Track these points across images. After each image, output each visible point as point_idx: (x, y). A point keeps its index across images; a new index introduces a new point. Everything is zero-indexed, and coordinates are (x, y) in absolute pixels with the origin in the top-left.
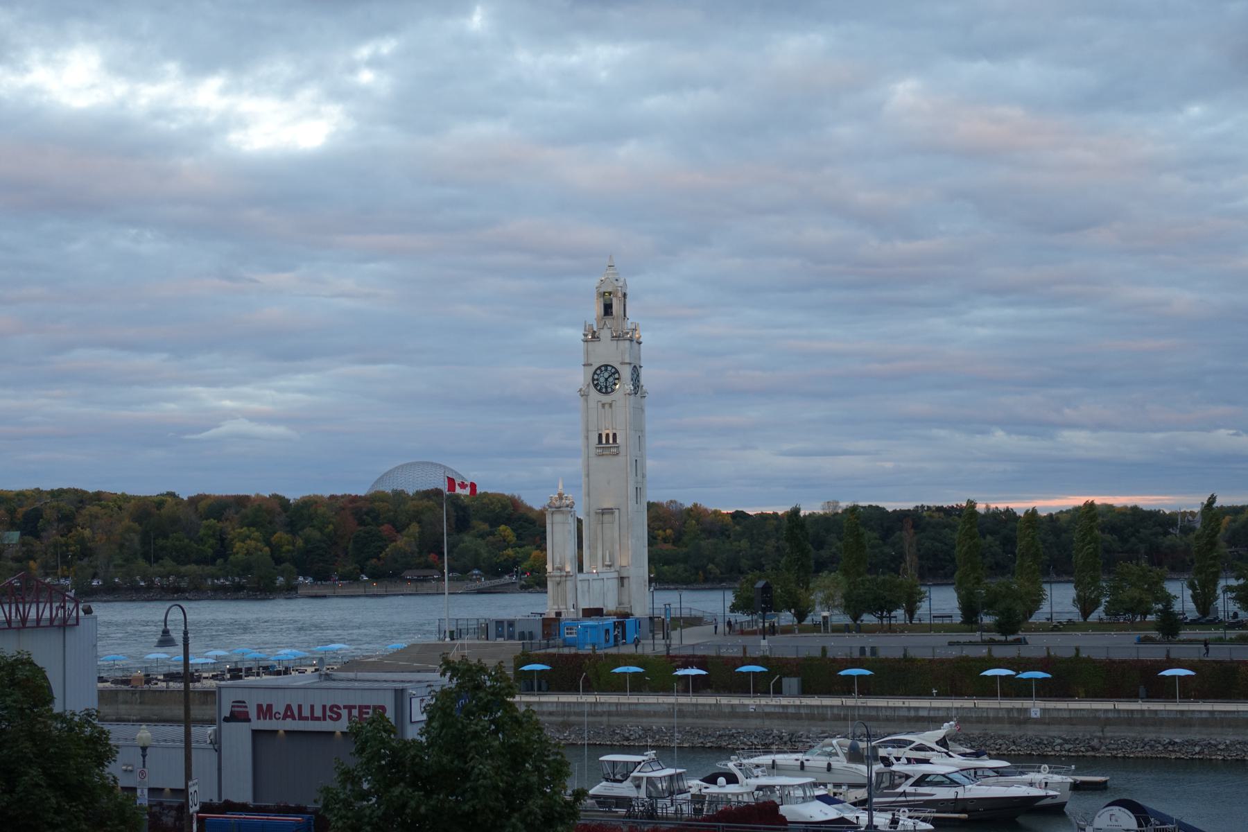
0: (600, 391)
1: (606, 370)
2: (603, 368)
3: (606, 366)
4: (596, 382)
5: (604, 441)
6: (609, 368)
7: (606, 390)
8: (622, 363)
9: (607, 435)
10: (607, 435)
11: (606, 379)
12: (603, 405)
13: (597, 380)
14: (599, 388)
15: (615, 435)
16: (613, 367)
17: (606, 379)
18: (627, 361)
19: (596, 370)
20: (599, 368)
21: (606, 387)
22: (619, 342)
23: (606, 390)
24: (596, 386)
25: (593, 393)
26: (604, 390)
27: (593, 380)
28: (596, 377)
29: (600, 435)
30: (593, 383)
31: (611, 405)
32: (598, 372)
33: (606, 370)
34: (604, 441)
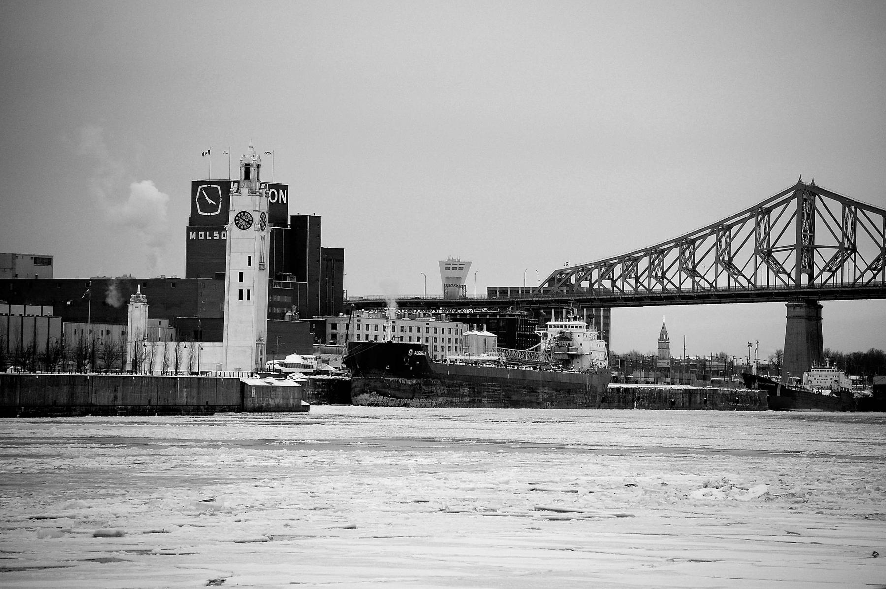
0: (239, 228)
1: (244, 215)
2: (242, 213)
3: (244, 212)
4: (237, 222)
6: (246, 214)
7: (243, 227)
8: (254, 211)
11: (244, 220)
14: (239, 226)
16: (248, 213)
18: (258, 209)
20: (240, 213)
21: (244, 226)
23: (243, 227)
24: (237, 224)
26: (242, 228)
27: (235, 220)
30: (235, 222)
33: (244, 215)
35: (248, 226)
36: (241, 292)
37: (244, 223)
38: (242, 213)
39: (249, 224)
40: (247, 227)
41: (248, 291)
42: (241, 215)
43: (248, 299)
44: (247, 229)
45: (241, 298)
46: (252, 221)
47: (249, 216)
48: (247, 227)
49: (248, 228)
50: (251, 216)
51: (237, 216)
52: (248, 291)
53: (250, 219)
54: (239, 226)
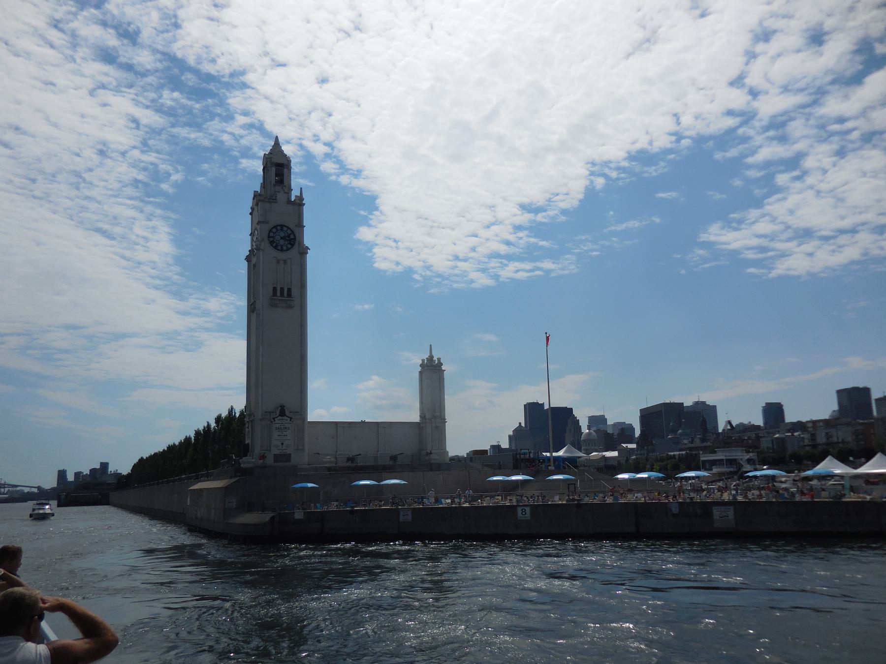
0: (275, 248)
1: (282, 230)
3: (282, 226)
4: (271, 239)
5: (278, 294)
6: (285, 229)
7: (282, 248)
9: (282, 289)
10: (282, 289)
12: (278, 261)
13: (272, 237)
14: (274, 245)
15: (289, 290)
16: (288, 228)
19: (273, 228)
20: (275, 227)
21: (282, 246)
24: (271, 243)
26: (279, 248)
27: (269, 237)
28: (271, 234)
29: (275, 289)
31: (285, 262)
33: (282, 230)
34: (278, 294)
35: (289, 246)
37: (282, 242)
39: (290, 243)
40: (287, 247)
42: (277, 230)
44: (286, 250)
46: (295, 239)
47: (289, 232)
49: (288, 249)
51: (270, 231)
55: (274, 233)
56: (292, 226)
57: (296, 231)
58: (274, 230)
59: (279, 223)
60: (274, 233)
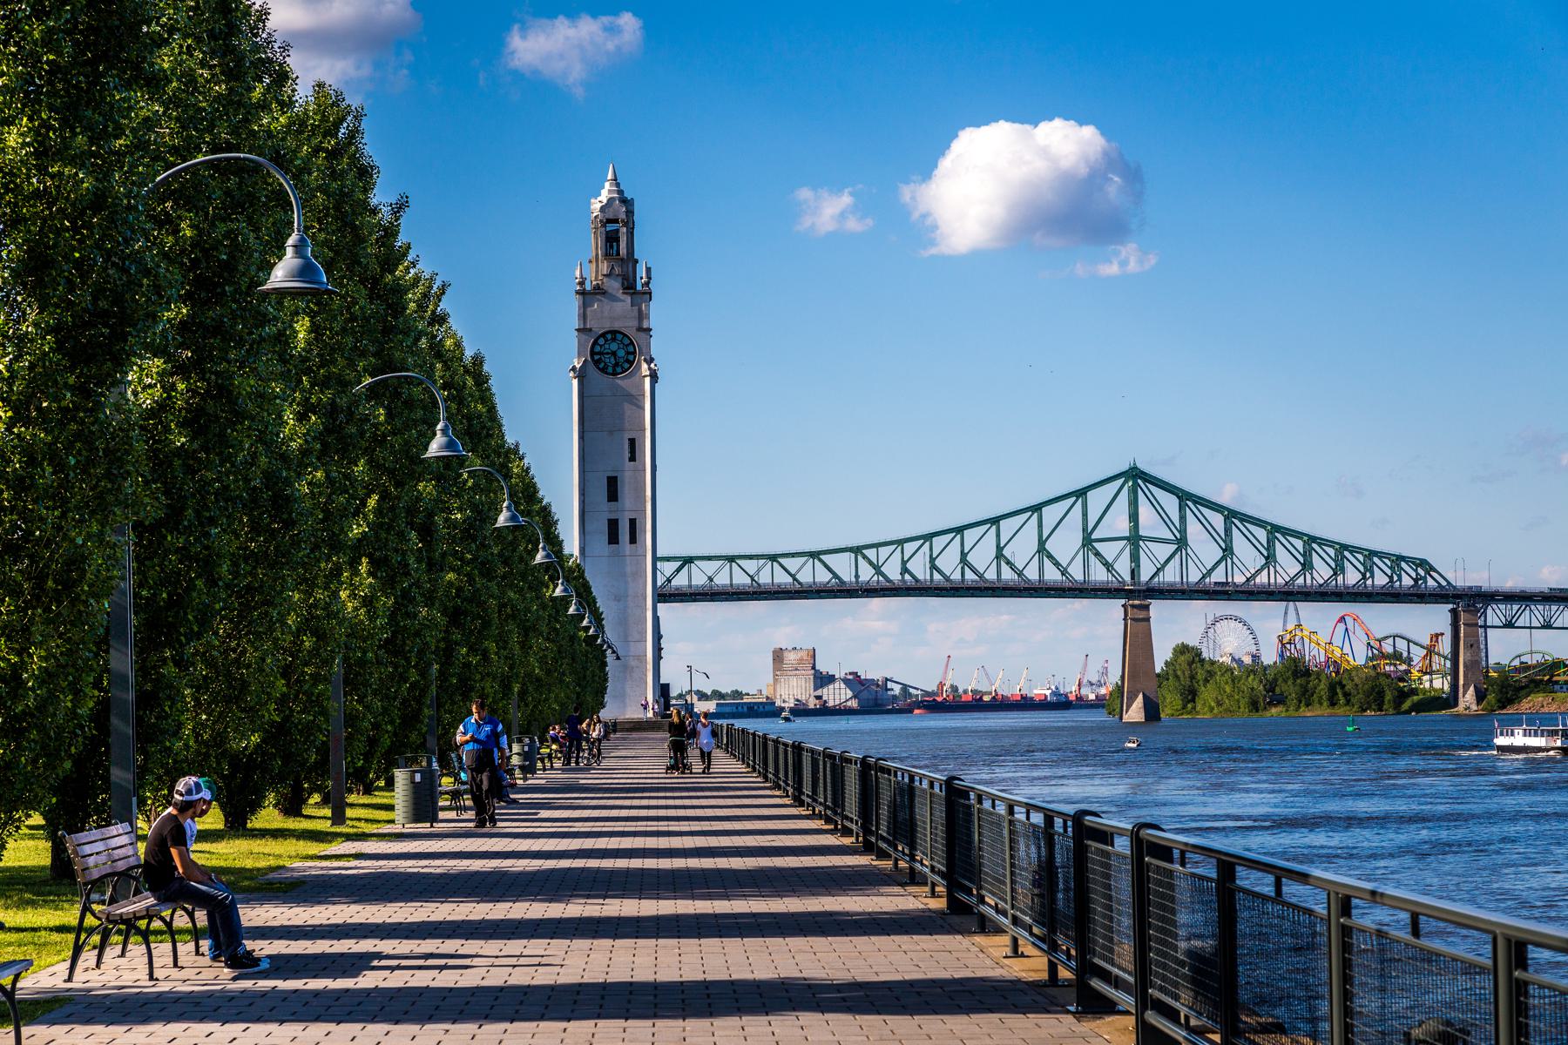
1: (614, 339)
2: (609, 336)
3: (614, 332)
4: (596, 357)
6: (619, 337)
14: (602, 366)
16: (625, 335)
17: (614, 354)
20: (603, 335)
22: (634, 296)
25: (593, 371)
26: (610, 370)
28: (598, 349)
32: (601, 341)
36: (613, 525)
38: (609, 336)
40: (622, 368)
41: (633, 522)
42: (606, 340)
43: (633, 540)
45: (613, 538)
47: (626, 341)
48: (622, 368)
50: (632, 343)
51: (595, 343)
52: (633, 522)
53: (631, 349)
54: (602, 366)
55: (601, 346)
56: (631, 333)
57: (637, 337)
58: (601, 341)
59: (607, 326)
60: (601, 346)
